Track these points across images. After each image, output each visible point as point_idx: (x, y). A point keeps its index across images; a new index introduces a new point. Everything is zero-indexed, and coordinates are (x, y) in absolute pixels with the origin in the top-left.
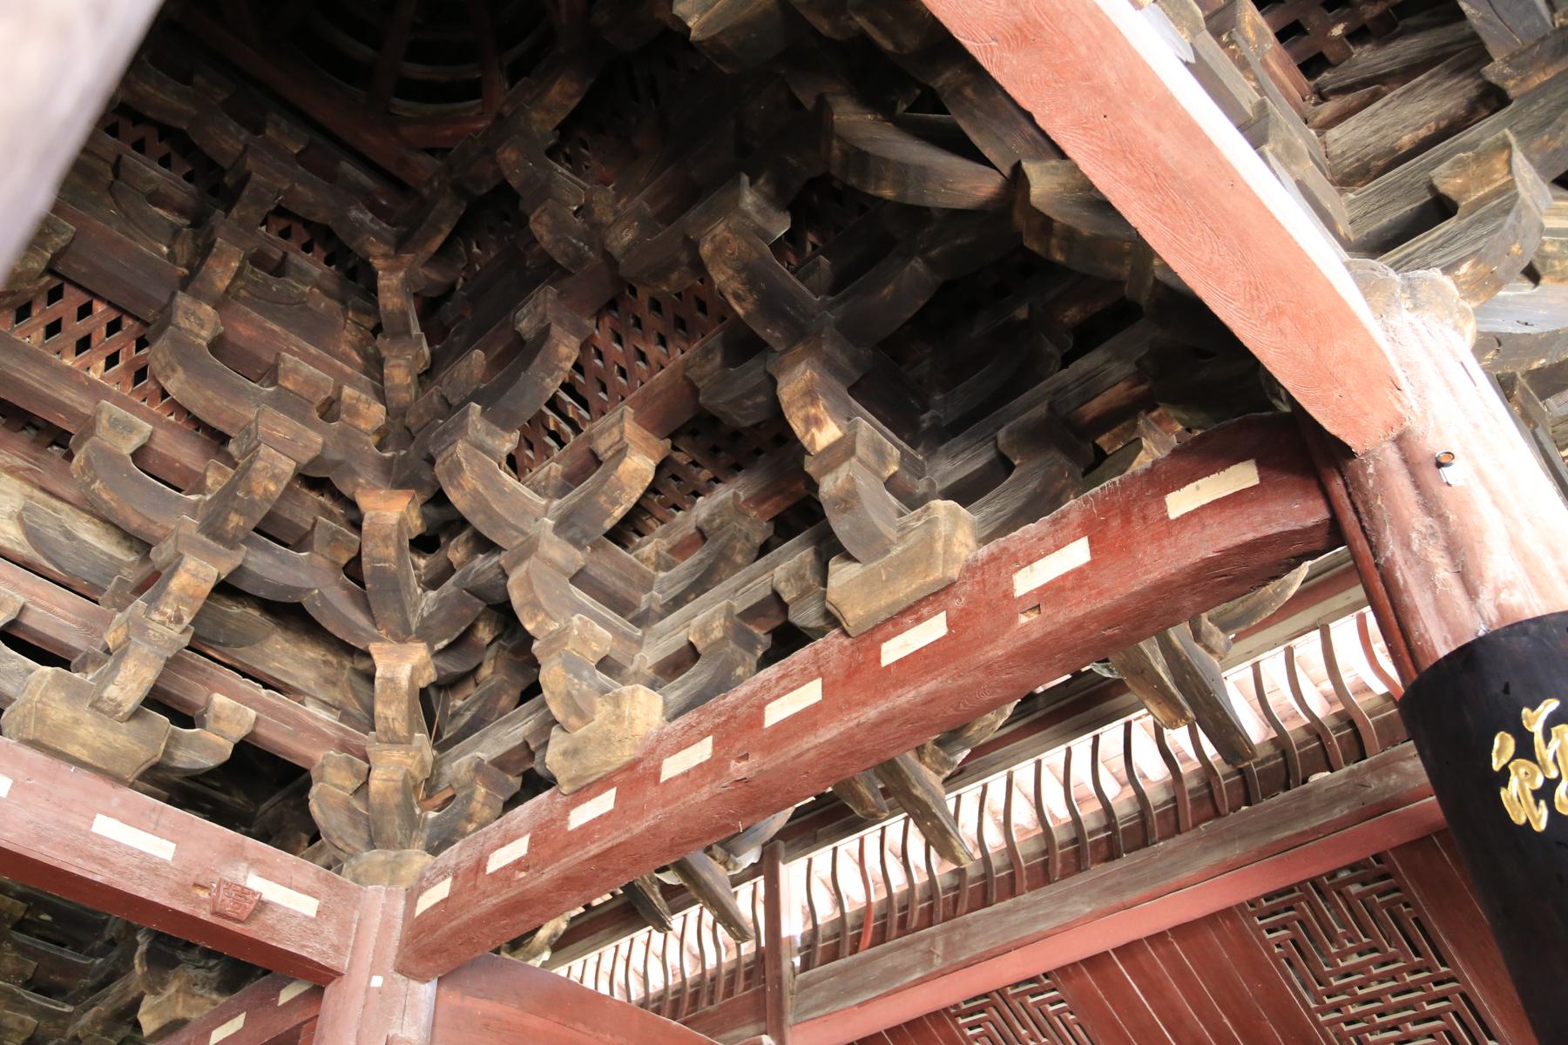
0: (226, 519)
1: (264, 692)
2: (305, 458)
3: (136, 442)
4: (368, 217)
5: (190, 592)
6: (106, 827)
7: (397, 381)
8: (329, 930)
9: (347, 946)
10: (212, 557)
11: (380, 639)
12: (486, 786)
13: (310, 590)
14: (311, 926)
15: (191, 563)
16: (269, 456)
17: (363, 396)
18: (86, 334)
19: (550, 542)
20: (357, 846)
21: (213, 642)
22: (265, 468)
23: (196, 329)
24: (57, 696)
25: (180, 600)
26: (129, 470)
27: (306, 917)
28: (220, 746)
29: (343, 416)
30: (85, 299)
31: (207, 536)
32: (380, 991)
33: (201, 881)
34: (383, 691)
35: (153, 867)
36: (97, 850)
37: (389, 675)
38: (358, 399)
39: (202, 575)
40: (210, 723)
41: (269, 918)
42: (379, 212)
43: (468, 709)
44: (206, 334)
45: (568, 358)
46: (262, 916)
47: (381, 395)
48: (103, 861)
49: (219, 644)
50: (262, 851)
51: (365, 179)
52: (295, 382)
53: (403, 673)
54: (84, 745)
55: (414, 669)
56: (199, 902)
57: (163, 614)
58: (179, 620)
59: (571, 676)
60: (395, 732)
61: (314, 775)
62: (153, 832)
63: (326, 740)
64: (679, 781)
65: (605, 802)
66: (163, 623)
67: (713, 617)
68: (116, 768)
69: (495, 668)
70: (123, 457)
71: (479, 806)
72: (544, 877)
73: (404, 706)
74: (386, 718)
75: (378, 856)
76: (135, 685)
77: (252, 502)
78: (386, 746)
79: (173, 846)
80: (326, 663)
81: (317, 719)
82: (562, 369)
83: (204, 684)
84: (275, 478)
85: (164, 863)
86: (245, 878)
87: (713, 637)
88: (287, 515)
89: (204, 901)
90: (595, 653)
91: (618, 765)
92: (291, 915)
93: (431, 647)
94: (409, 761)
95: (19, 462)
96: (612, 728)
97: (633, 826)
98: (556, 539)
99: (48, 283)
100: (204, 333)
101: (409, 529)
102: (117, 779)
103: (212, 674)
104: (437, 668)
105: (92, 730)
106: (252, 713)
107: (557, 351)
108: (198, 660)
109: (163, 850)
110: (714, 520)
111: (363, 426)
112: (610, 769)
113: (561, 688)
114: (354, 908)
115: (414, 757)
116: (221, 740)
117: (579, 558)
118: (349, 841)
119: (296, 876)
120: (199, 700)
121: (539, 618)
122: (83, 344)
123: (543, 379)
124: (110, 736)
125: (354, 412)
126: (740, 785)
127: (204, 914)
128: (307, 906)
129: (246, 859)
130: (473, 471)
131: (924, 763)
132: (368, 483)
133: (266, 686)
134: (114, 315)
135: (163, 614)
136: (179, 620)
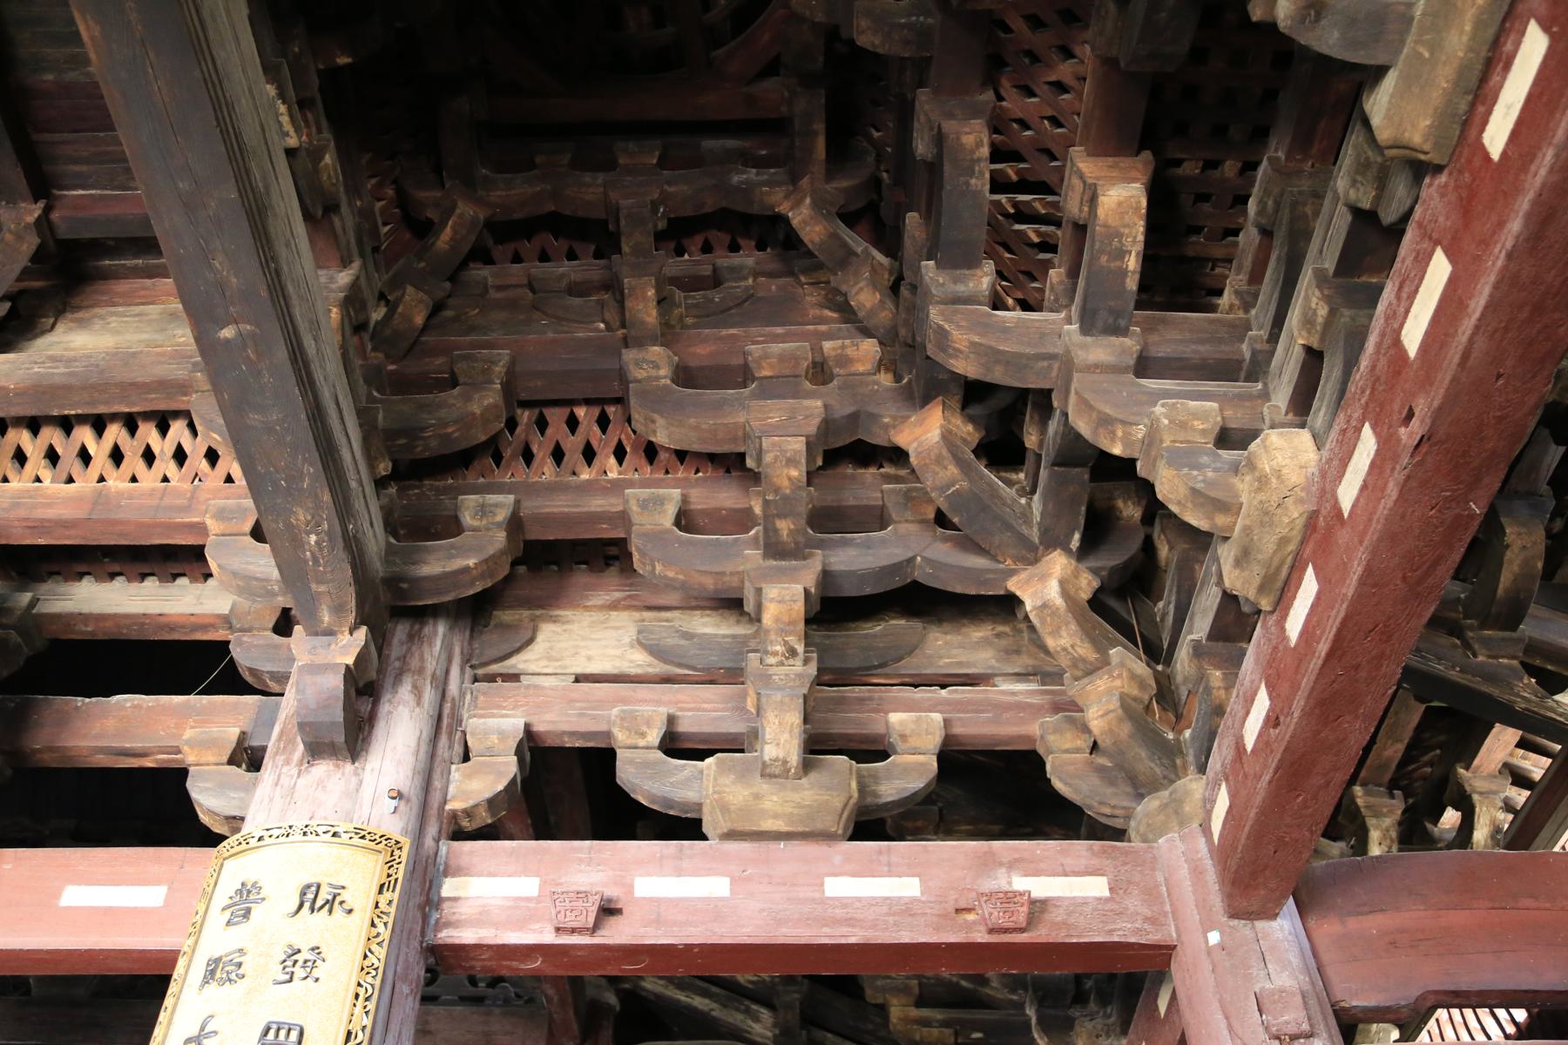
0: (776, 531)
1: (943, 692)
2: (812, 427)
3: (671, 511)
4: (752, 174)
5: (786, 619)
6: (839, 887)
7: (868, 305)
8: (1134, 903)
9: (1165, 914)
10: (790, 576)
11: (1012, 573)
12: (1217, 667)
13: (914, 558)
14: (1109, 906)
15: (772, 592)
16: (774, 445)
17: (847, 342)
18: (585, 442)
19: (1083, 346)
20: (1125, 803)
21: (868, 668)
22: (776, 458)
23: (653, 373)
24: (727, 780)
25: (782, 632)
26: (678, 539)
27: (1100, 899)
28: (922, 764)
29: (837, 370)
30: (565, 412)
31: (775, 559)
32: (1222, 947)
33: (963, 904)
34: (1043, 622)
35: (906, 909)
36: (839, 912)
37: (1039, 603)
38: (843, 347)
39: (788, 598)
40: (900, 746)
41: (1057, 915)
42: (760, 163)
43: (1169, 603)
44: (664, 371)
45: (979, 144)
46: (1047, 916)
47: (867, 333)
48: (850, 922)
49: (876, 667)
50: (1016, 850)
51: (731, 143)
52: (771, 366)
53: (1053, 591)
54: (776, 816)
55: (1062, 583)
56: (969, 926)
57: (775, 654)
58: (793, 652)
59: (1186, 470)
60: (1084, 660)
61: (1041, 751)
62: (890, 874)
63: (1037, 710)
64: (1361, 500)
65: (1309, 586)
66: (781, 664)
67: (1307, 299)
68: (819, 826)
69: (1169, 542)
70: (668, 531)
71: (1222, 692)
72: (1296, 715)
73: (1073, 627)
74: (1065, 649)
75: (1151, 803)
76: (786, 736)
77: (785, 498)
78: (1086, 680)
79: (916, 880)
80: (998, 635)
81: (1014, 693)
82: (979, 160)
83: (877, 711)
84: (791, 462)
85: (914, 900)
86: (1010, 883)
87: (1320, 320)
88: (852, 502)
89: (974, 922)
90: (1204, 432)
91: (1296, 535)
92: (1079, 904)
93: (1067, 550)
94: (1118, 683)
95: (617, 595)
96: (1262, 496)
97: (1344, 591)
98: (1089, 339)
99: (529, 418)
100: (662, 372)
101: (964, 441)
102: (826, 836)
103: (881, 698)
104: (1094, 571)
105: (775, 798)
106: (937, 717)
107: (962, 145)
108: (860, 691)
109: (907, 887)
110: (1266, 203)
111: (861, 369)
112: (1292, 547)
113: (1183, 491)
114: (1153, 869)
115: (1120, 676)
116: (921, 758)
117: (1129, 345)
118: (1113, 802)
119: (1068, 861)
120: (879, 729)
121: (1120, 433)
122: (589, 454)
123: (967, 184)
124: (796, 797)
125: (844, 361)
126: (1424, 449)
127: (981, 937)
128: (1096, 887)
129: (1001, 864)
130: (959, 327)
132: (894, 418)
133: (943, 687)
134: (596, 411)
135: (775, 654)
136: (793, 652)
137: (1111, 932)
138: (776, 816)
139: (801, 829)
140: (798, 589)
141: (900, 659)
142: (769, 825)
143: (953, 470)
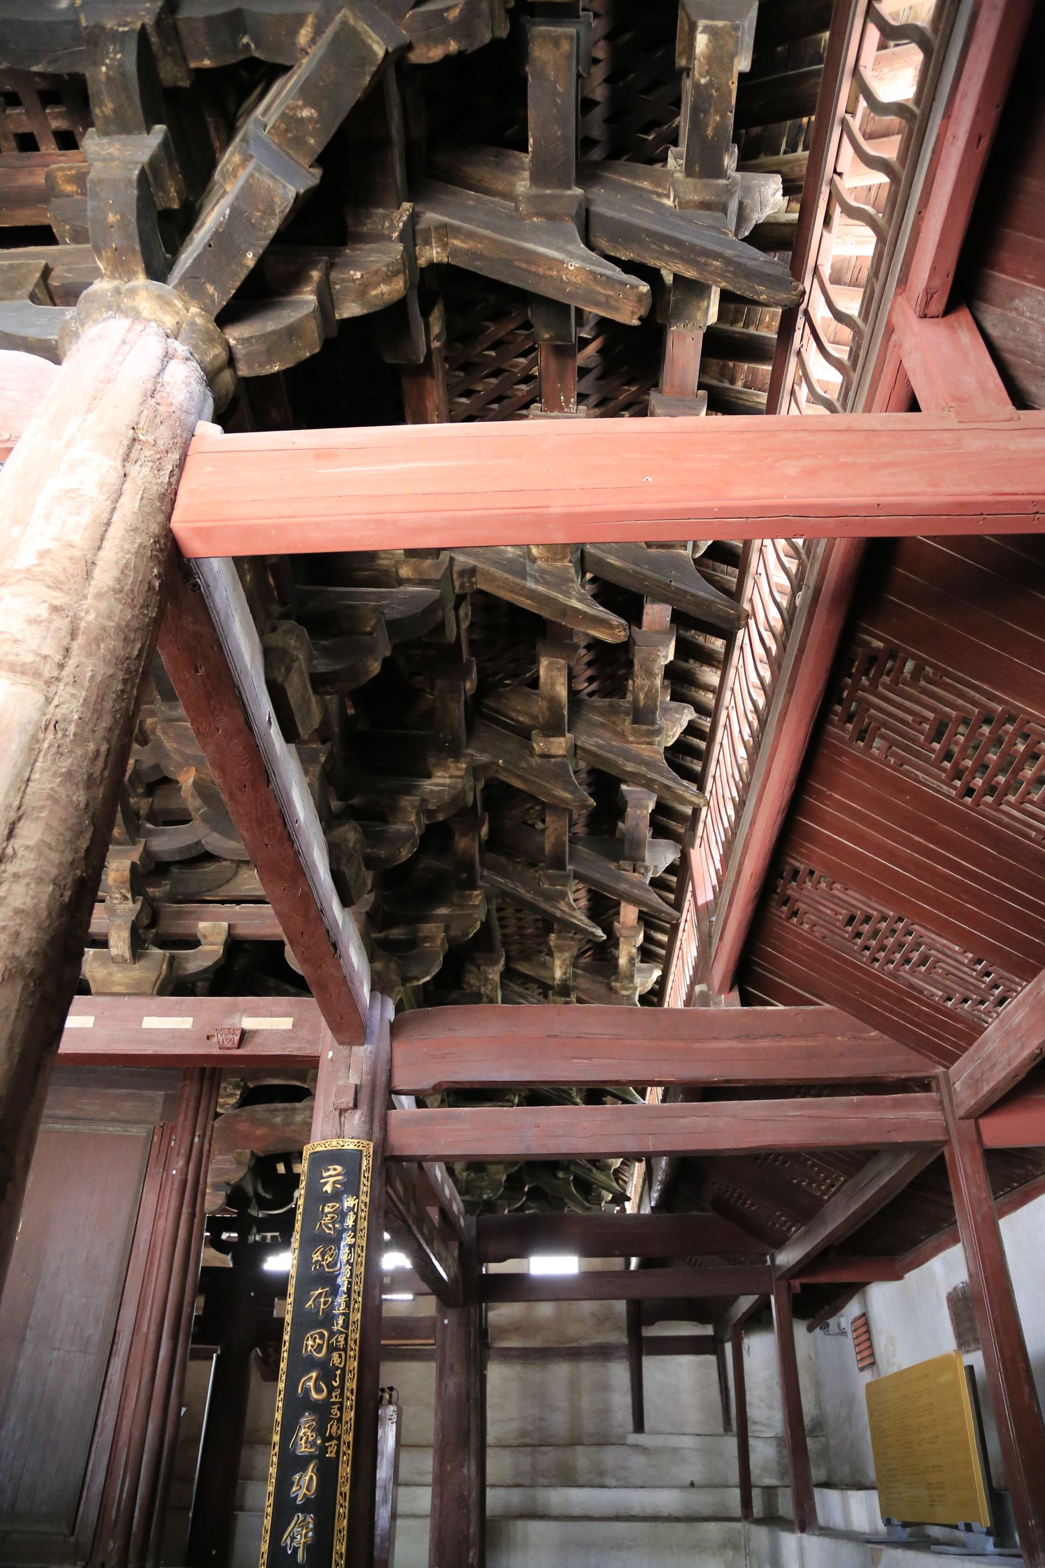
6: (150, 1022)
8: (303, 1033)
14: (290, 1034)
27: (284, 1031)
40: (203, 941)
54: (120, 984)
57: (117, 898)
58: (126, 898)
62: (179, 1016)
66: (121, 903)
76: (121, 943)
79: (191, 1019)
85: (187, 1030)
92: (272, 1033)
102: (152, 994)
106: (225, 924)
109: (185, 1023)
124: (131, 974)
127: (216, 1051)
128: (285, 1023)
131: (632, 743)
135: (117, 898)
137: (284, 1049)
138: (120, 984)
139: (133, 991)
140: (128, 863)
141: (220, 886)
142: (116, 989)
143: (198, 802)
